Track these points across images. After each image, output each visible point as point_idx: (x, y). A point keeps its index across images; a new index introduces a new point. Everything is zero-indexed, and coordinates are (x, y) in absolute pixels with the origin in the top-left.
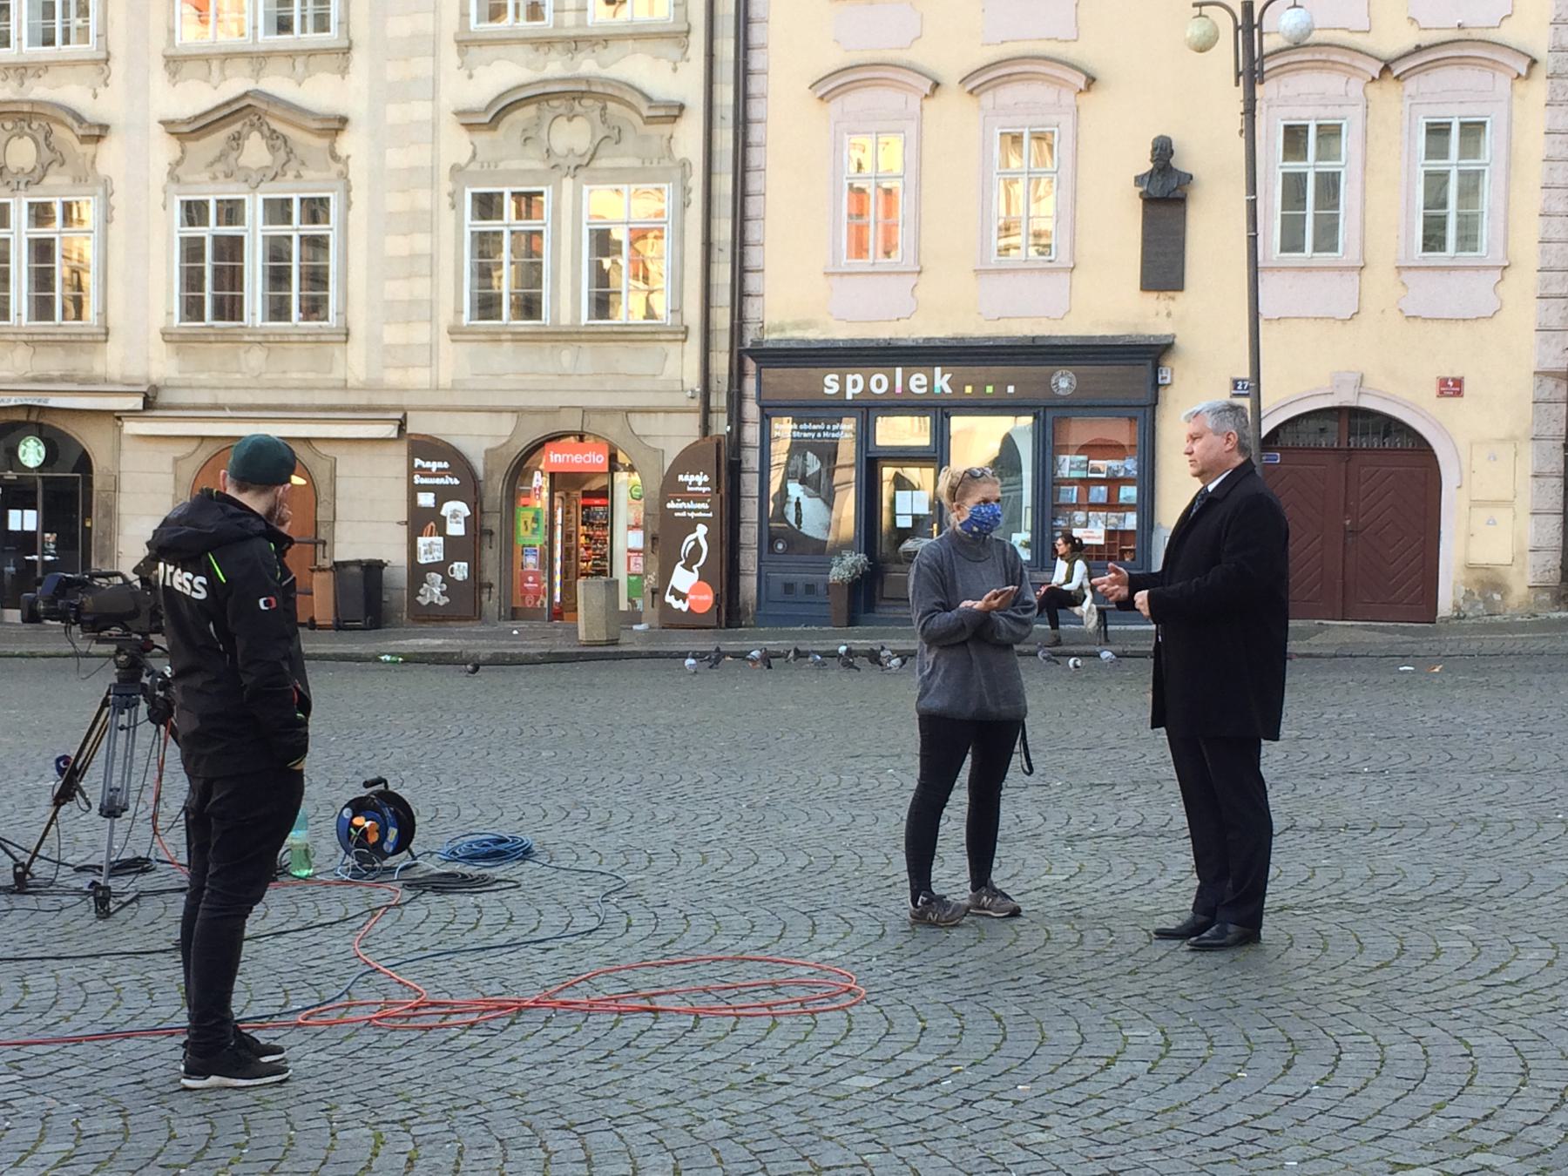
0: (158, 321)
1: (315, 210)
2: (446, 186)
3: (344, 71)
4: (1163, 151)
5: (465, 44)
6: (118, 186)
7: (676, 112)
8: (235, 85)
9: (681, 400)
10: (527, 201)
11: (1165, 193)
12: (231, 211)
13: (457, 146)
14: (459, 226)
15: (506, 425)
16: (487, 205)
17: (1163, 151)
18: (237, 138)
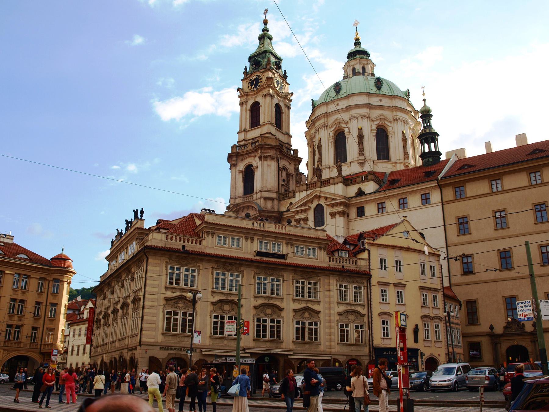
0: (291, 340)
1: (316, 324)
2: (336, 323)
3: (319, 305)
4: (417, 326)
5: (338, 303)
6: (285, 318)
7: (364, 315)
8: (303, 305)
9: (367, 354)
10: (347, 326)
11: (416, 331)
12: (303, 323)
13: (337, 317)
14: (338, 329)
15: (345, 357)
16: (342, 326)
17: (417, 326)
18: (304, 313)
